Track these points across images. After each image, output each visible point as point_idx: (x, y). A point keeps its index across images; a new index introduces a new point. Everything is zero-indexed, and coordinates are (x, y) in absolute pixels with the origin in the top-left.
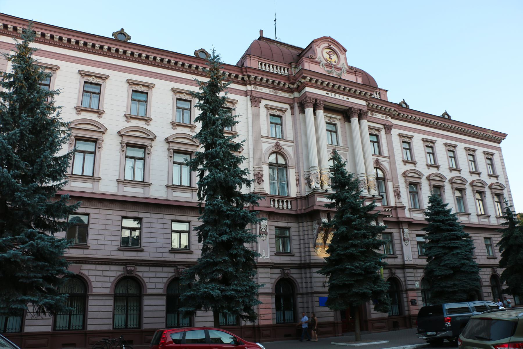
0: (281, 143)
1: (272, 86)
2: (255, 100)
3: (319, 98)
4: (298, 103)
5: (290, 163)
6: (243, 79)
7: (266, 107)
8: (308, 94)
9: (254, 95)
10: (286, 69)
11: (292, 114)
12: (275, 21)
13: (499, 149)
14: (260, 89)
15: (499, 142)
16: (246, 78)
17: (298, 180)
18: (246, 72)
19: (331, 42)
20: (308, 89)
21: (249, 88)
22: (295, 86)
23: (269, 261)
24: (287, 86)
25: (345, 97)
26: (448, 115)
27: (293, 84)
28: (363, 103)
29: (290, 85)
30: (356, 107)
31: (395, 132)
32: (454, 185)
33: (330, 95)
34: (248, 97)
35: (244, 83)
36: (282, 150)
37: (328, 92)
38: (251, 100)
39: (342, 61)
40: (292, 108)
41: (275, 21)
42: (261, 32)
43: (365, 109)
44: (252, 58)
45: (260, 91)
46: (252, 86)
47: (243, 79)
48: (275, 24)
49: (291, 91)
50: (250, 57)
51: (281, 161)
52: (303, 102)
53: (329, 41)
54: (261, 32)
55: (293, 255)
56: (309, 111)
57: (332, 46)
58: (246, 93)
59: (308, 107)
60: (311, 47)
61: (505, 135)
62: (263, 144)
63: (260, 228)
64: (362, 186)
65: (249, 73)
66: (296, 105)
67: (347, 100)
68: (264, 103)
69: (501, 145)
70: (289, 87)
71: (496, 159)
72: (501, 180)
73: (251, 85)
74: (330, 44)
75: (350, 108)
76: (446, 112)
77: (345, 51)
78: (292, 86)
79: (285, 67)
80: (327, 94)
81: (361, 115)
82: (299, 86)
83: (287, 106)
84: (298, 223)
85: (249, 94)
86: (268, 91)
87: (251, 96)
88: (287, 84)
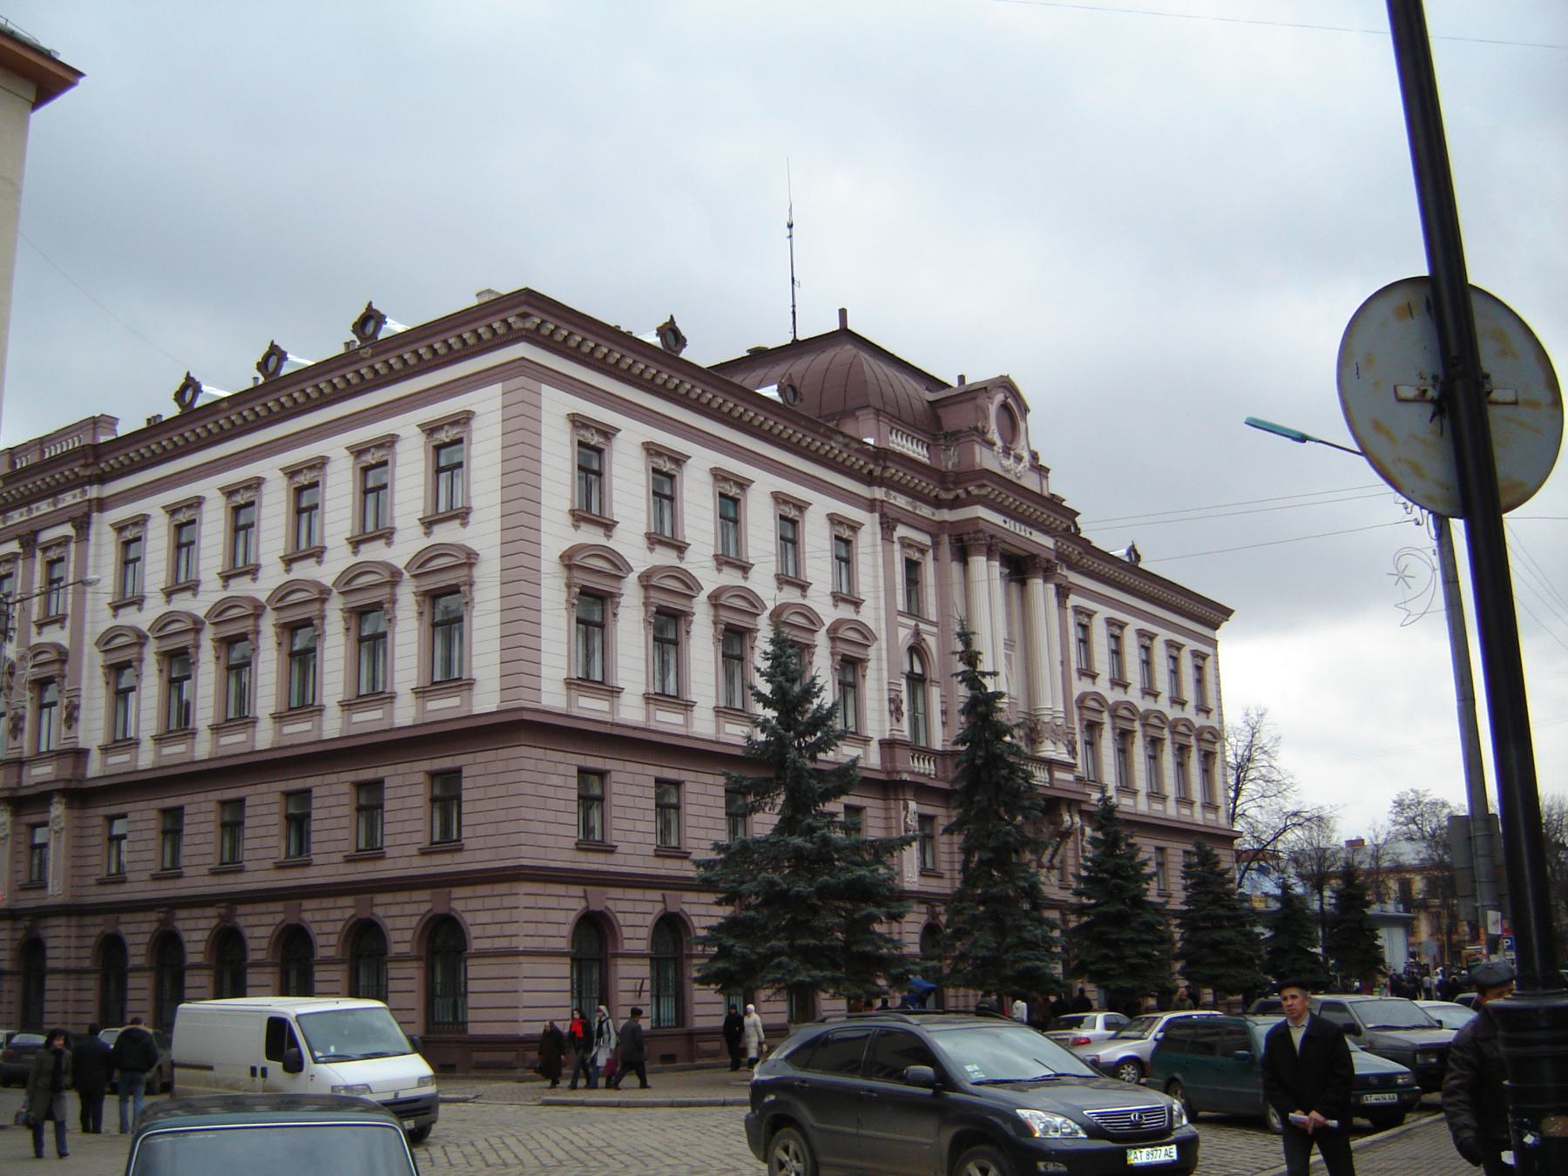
0: (922, 626)
1: (915, 495)
2: (888, 526)
3: (999, 535)
4: (950, 536)
5: (934, 672)
6: (871, 472)
7: (902, 540)
8: (982, 525)
9: (892, 514)
10: (925, 445)
11: (936, 559)
12: (790, 226)
13: (1213, 643)
14: (895, 498)
15: (1215, 626)
16: (877, 472)
17: (944, 713)
18: (885, 460)
19: (1008, 389)
20: (981, 512)
21: (879, 493)
22: (951, 496)
23: (915, 887)
24: (934, 494)
25: (1028, 530)
26: (1135, 552)
27: (948, 490)
28: (1049, 542)
29: (941, 492)
30: (1044, 555)
31: (1074, 600)
32: (1149, 729)
33: (1007, 526)
34: (877, 515)
35: (870, 480)
36: (923, 644)
37: (1008, 520)
38: (881, 524)
39: (1023, 442)
40: (936, 544)
41: (790, 226)
42: (843, 313)
43: (1053, 558)
44: (881, 418)
45: (892, 501)
46: (884, 489)
47: (871, 472)
48: (791, 236)
49: (938, 504)
50: (878, 415)
51: (918, 669)
52: (965, 537)
53: (1005, 387)
54: (843, 313)
55: (940, 876)
56: (979, 564)
57: (1009, 400)
58: (871, 505)
59: (979, 553)
60: (974, 399)
61: (1227, 613)
62: (900, 629)
63: (906, 817)
64: (1046, 735)
65: (888, 464)
66: (945, 539)
67: (1028, 536)
68: (901, 531)
69: (1219, 635)
70: (936, 496)
71: (1209, 663)
72: (1212, 721)
73: (880, 486)
74: (1008, 395)
75: (1033, 556)
76: (1133, 546)
77: (1027, 410)
78: (944, 495)
79: (920, 437)
80: (1005, 522)
81: (1048, 573)
82: (957, 497)
83: (925, 539)
84: (947, 808)
85: (877, 508)
86: (904, 502)
87: (882, 516)
88: (937, 489)
